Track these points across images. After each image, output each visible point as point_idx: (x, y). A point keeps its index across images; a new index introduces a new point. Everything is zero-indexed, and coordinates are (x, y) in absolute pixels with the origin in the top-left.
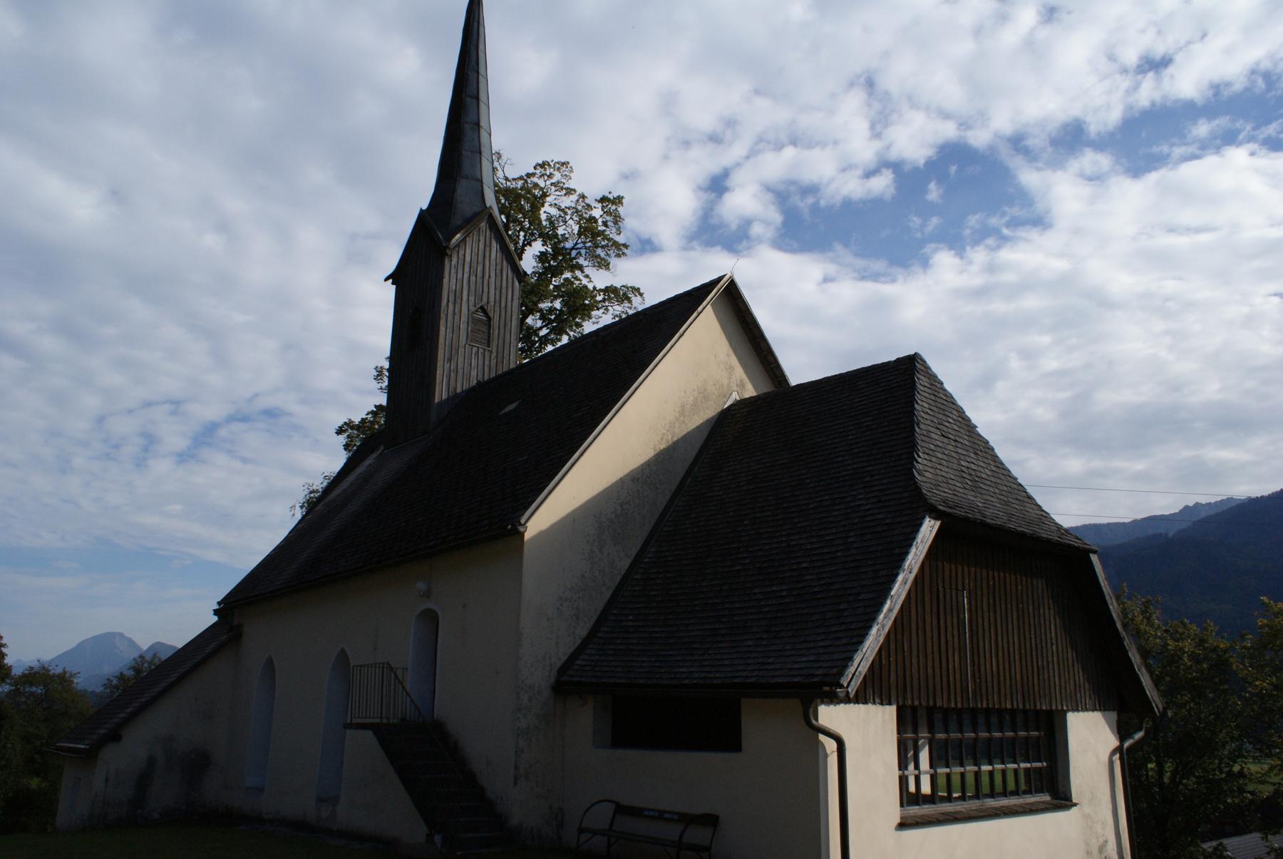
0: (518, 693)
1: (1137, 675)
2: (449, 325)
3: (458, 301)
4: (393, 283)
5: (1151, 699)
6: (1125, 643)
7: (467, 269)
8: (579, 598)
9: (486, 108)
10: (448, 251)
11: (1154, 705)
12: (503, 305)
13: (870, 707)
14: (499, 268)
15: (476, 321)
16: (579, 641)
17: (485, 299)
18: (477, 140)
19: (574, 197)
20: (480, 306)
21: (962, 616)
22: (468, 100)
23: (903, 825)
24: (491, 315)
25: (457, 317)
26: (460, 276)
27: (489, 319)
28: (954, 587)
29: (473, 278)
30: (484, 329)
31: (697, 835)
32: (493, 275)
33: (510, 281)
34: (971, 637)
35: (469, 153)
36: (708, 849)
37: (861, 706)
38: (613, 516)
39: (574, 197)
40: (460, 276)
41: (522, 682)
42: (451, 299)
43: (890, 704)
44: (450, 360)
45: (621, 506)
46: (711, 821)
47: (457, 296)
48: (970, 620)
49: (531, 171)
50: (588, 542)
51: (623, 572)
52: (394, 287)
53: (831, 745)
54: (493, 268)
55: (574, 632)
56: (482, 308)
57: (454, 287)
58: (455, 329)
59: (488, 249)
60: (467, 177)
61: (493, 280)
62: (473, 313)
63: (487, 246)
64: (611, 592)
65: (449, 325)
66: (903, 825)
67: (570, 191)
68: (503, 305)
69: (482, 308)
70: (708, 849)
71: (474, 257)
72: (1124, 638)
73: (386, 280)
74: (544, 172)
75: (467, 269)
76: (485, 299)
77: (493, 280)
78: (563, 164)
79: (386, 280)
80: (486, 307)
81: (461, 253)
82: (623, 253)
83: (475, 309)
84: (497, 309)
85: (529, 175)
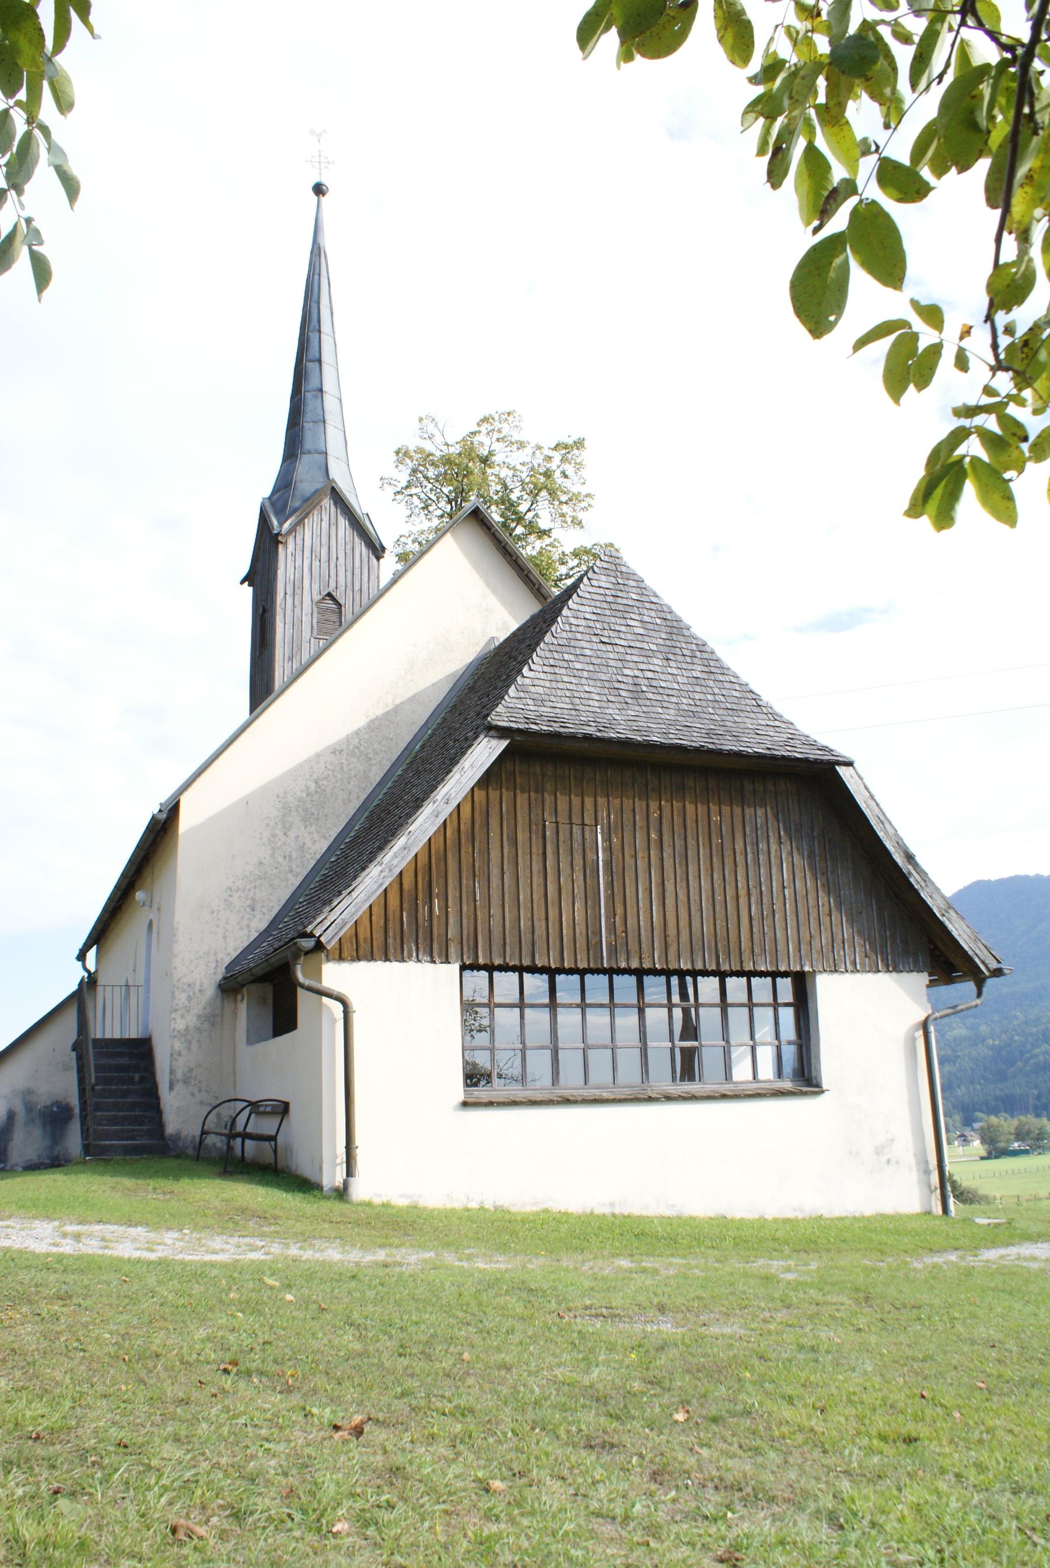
0: (173, 993)
1: (941, 924)
2: (289, 619)
3: (298, 591)
4: (249, 585)
5: (970, 953)
6: (912, 880)
7: (307, 554)
8: (255, 887)
9: (334, 370)
10: (280, 538)
11: (977, 960)
12: (357, 587)
13: (411, 966)
14: (349, 547)
15: (322, 612)
16: (257, 935)
17: (333, 585)
18: (320, 408)
19: (528, 450)
20: (326, 592)
21: (590, 856)
22: (310, 365)
23: (465, 1104)
24: (342, 602)
25: (298, 610)
26: (299, 562)
27: (339, 605)
28: (576, 819)
29: (316, 564)
30: (334, 618)
31: (267, 1126)
32: (341, 555)
33: (365, 559)
34: (610, 885)
35: (311, 424)
36: (273, 1138)
37: (396, 965)
38: (304, 795)
39: (528, 450)
40: (299, 562)
41: (179, 980)
42: (289, 591)
43: (447, 961)
44: (291, 659)
45: (316, 783)
46: (283, 1109)
47: (297, 587)
48: (609, 864)
49: (475, 428)
50: (267, 825)
51: (318, 856)
52: (251, 588)
53: (337, 1008)
54: (341, 548)
55: (248, 926)
56: (329, 595)
57: (292, 577)
58: (299, 622)
59: (333, 528)
60: (309, 452)
61: (341, 561)
62: (319, 602)
63: (333, 524)
64: (300, 879)
65: (289, 619)
66: (465, 1104)
67: (521, 445)
68: (357, 587)
69: (329, 595)
70: (273, 1138)
71: (317, 541)
72: (910, 873)
73: (242, 583)
74: (490, 428)
75: (307, 554)
76: (333, 585)
77: (341, 561)
78: (509, 414)
79: (242, 583)
80: (334, 594)
81: (299, 538)
82: (589, 505)
83: (320, 597)
84: (350, 593)
85: (474, 433)
